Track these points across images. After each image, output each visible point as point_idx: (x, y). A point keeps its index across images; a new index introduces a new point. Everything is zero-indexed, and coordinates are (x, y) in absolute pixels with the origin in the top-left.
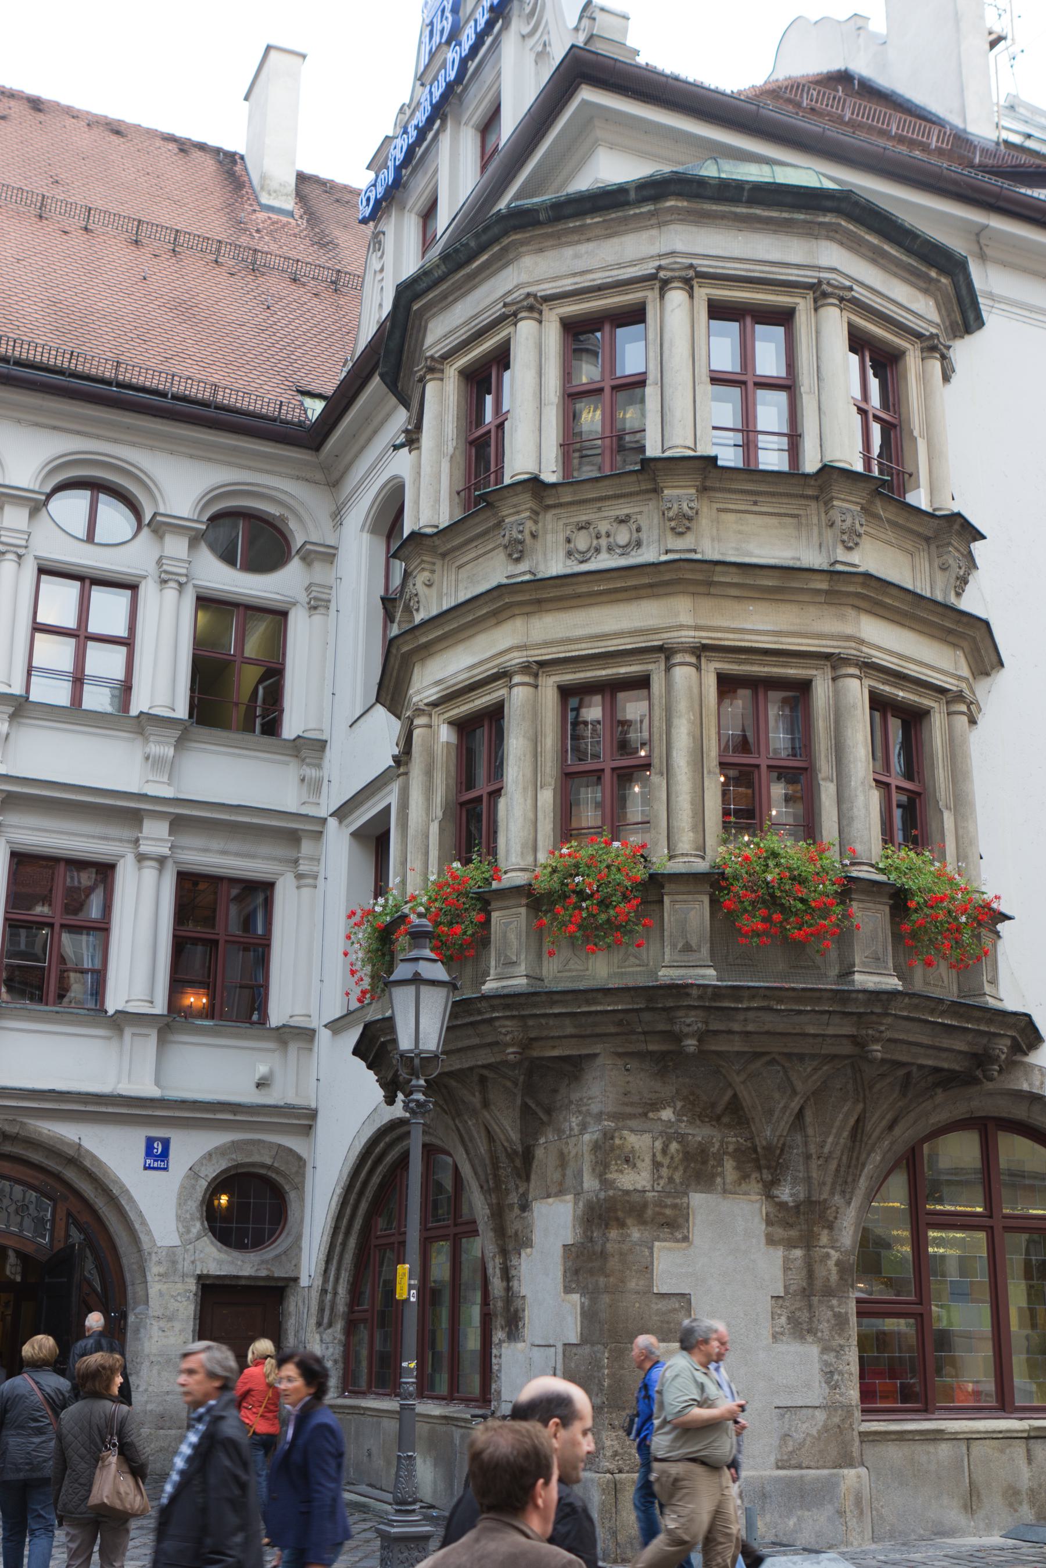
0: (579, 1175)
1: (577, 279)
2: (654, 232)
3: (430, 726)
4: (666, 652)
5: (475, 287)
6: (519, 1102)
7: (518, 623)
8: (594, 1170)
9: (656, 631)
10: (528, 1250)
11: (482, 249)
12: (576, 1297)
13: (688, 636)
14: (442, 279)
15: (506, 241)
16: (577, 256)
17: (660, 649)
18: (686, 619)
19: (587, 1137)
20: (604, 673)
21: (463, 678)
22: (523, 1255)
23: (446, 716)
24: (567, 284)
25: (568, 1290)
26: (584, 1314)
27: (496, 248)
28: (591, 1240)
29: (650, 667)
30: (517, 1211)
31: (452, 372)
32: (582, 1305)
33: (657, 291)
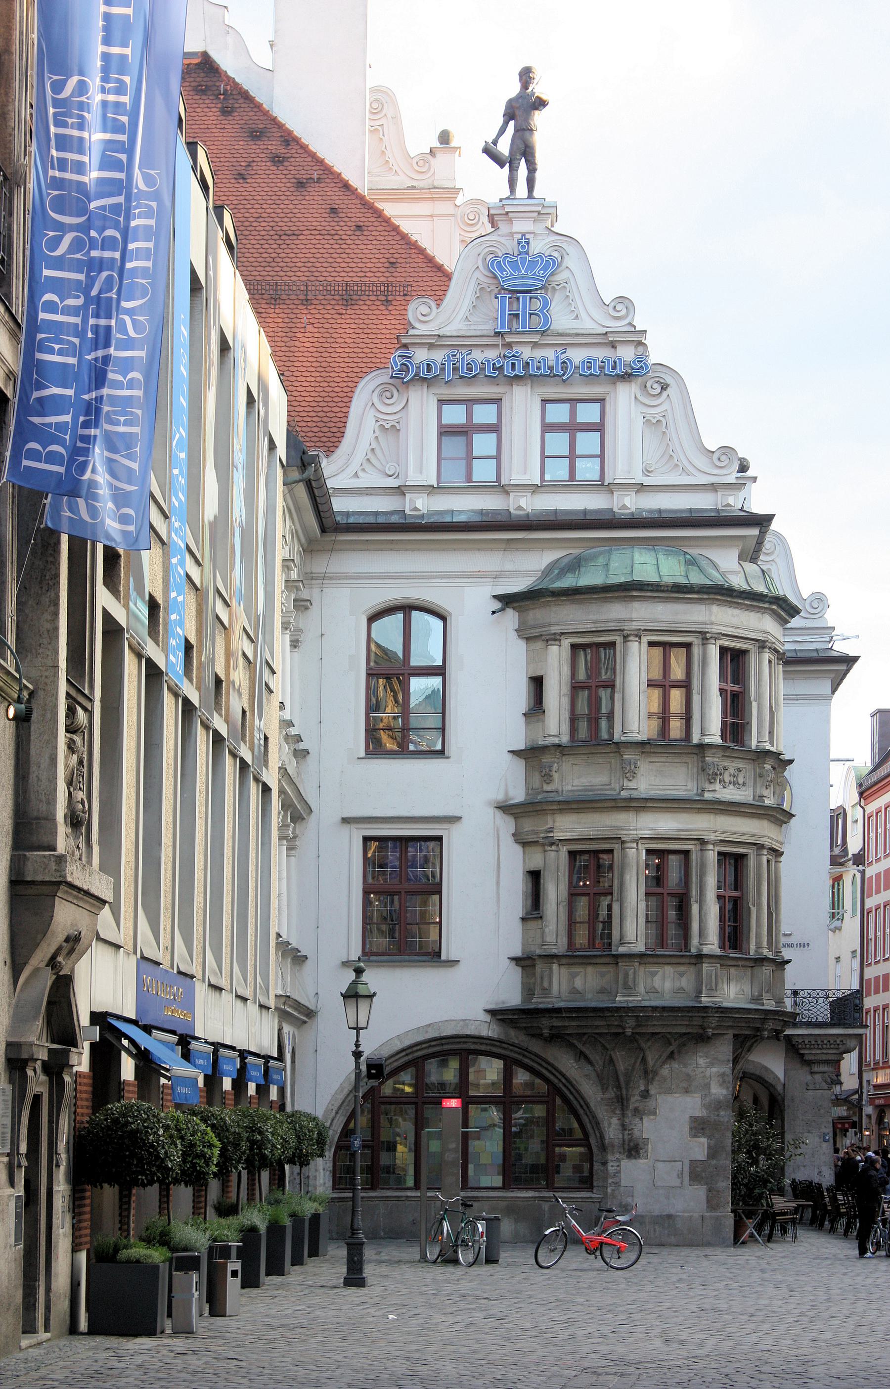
0: (707, 1086)
1: (733, 630)
2: (760, 615)
3: (637, 849)
4: (761, 847)
5: (675, 602)
6: (671, 1048)
7: (712, 817)
8: (721, 1085)
9: (759, 836)
10: (652, 1117)
11: (697, 593)
12: (704, 1140)
13: (767, 842)
14: (663, 591)
15: (712, 596)
16: (733, 616)
17: (755, 844)
18: (766, 833)
19: (714, 1070)
20: (735, 850)
21: (673, 834)
22: (645, 1119)
23: (647, 846)
24: (729, 631)
25: (695, 1136)
26: (709, 1147)
27: (705, 597)
28: (718, 1115)
29: (750, 851)
30: (637, 1097)
31: (645, 640)
32: (709, 1145)
33: (757, 648)
